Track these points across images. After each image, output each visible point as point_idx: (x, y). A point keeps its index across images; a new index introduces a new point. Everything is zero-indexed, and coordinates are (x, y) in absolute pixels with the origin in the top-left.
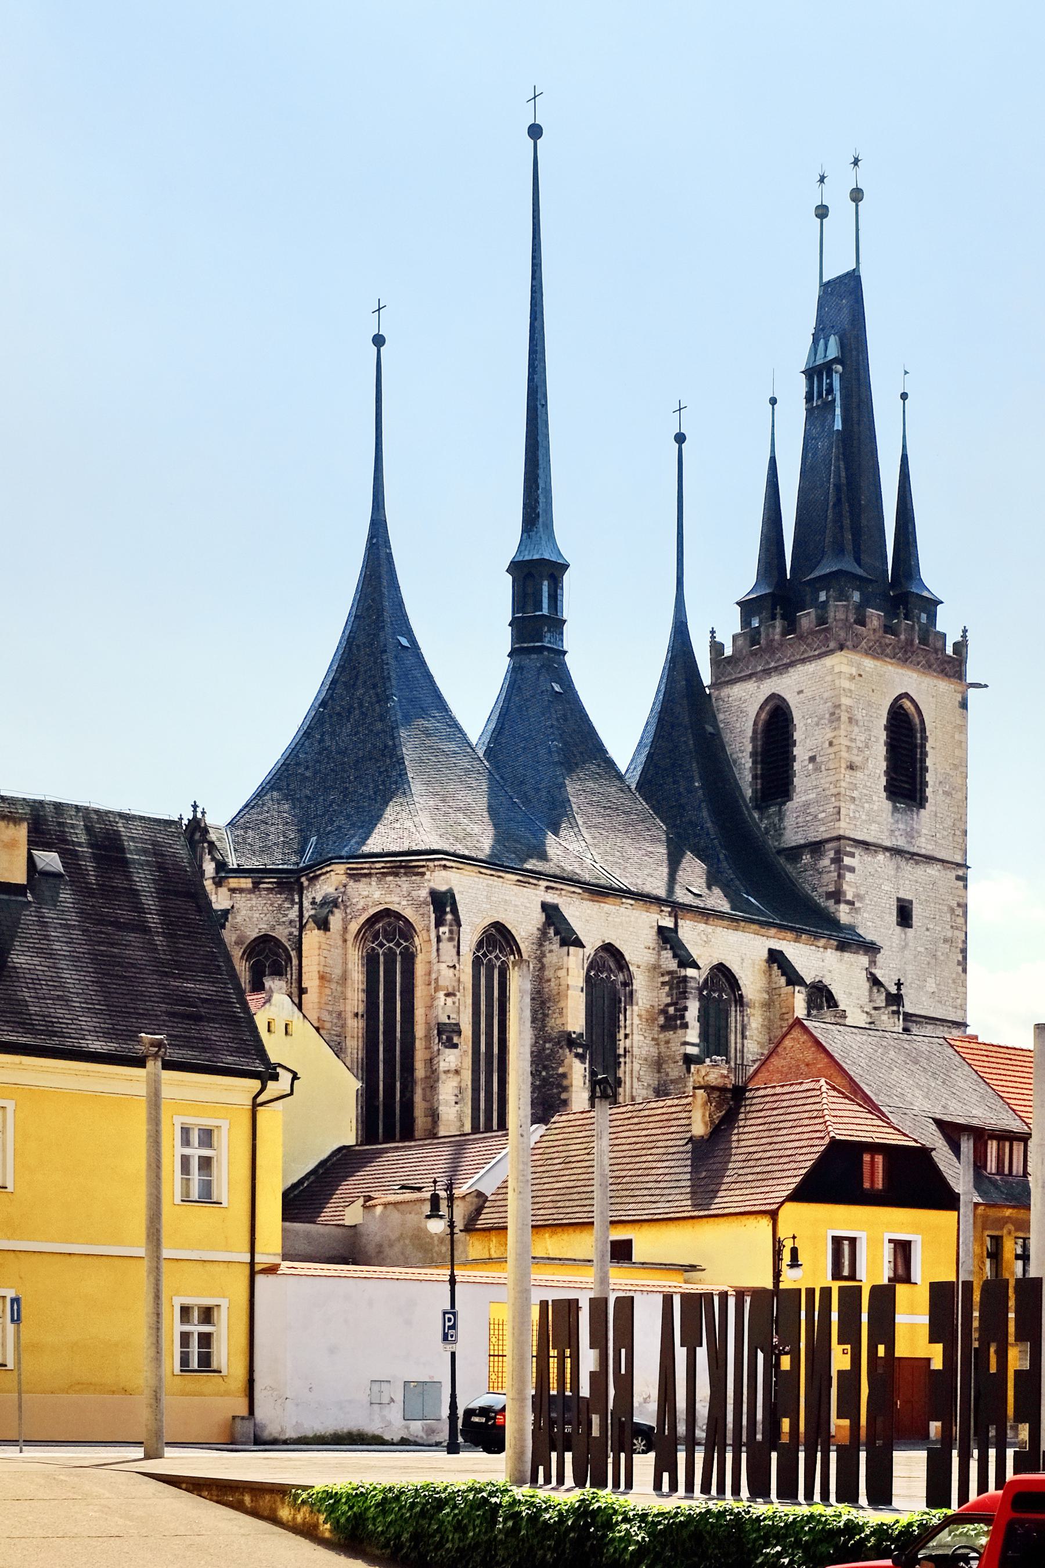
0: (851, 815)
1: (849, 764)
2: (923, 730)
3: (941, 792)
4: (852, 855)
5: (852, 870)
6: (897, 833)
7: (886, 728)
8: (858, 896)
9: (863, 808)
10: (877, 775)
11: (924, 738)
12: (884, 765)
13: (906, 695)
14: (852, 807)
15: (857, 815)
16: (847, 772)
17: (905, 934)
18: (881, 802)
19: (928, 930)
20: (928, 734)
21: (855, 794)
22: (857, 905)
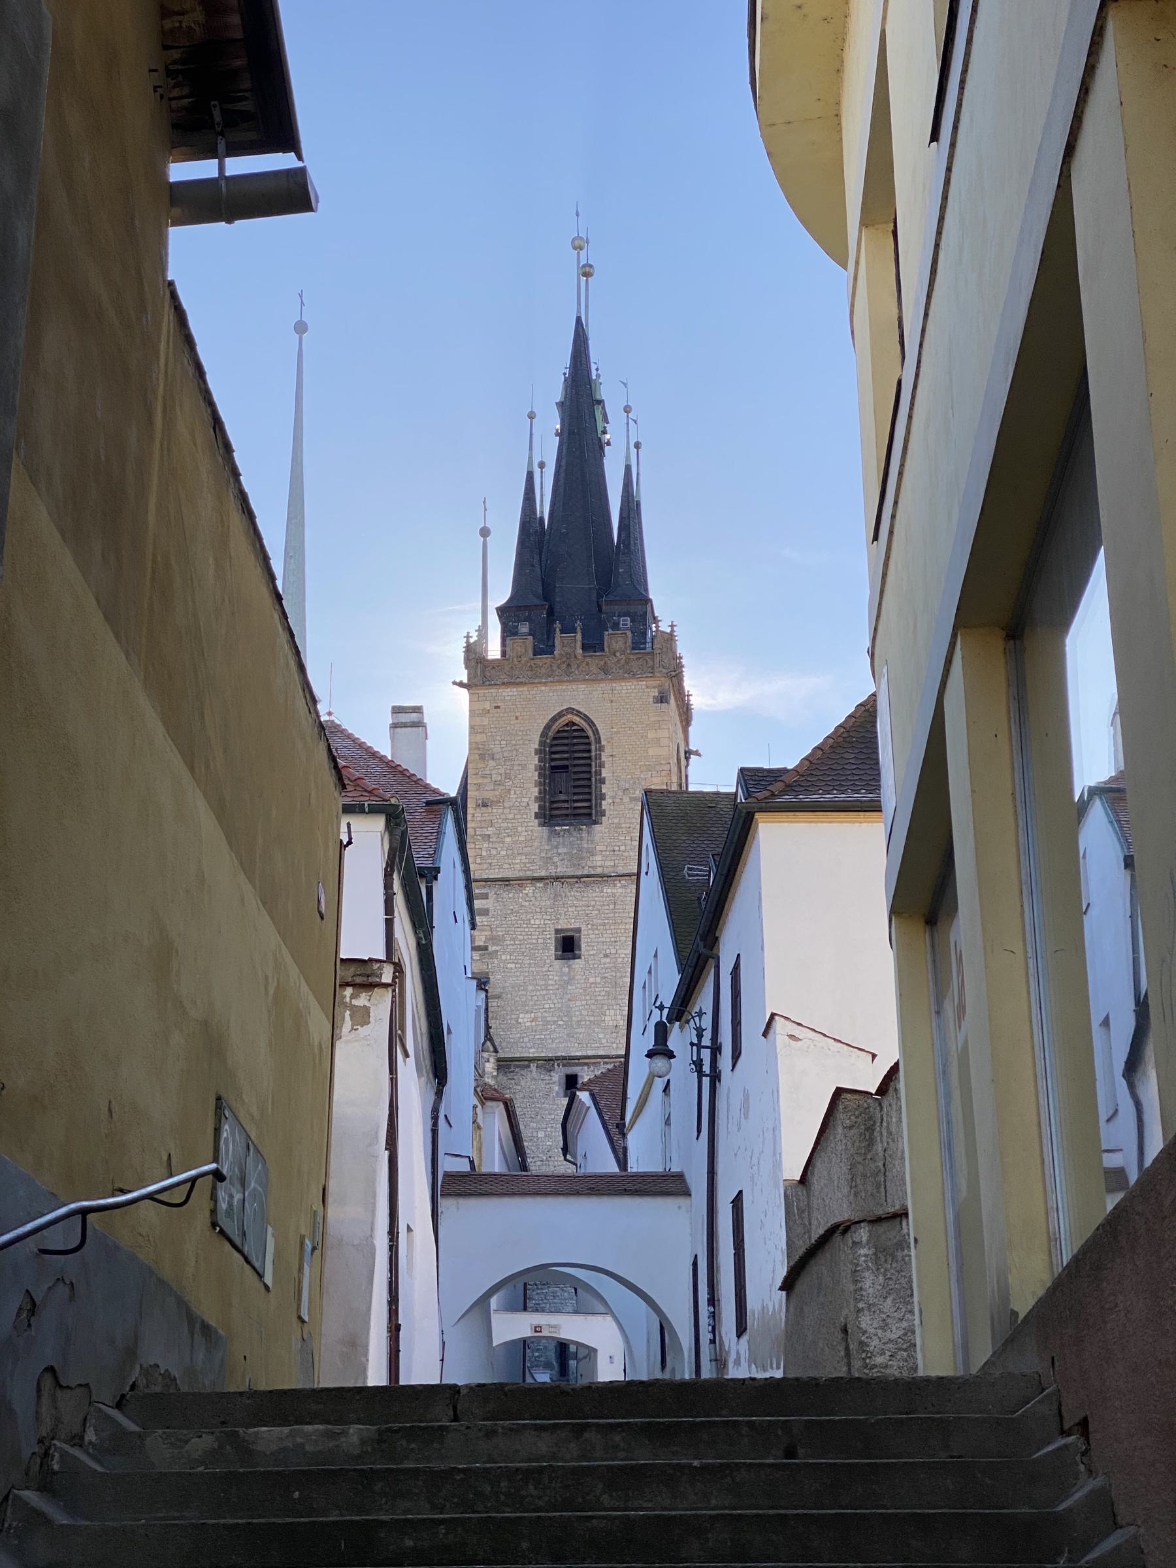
0: (484, 854)
1: (480, 802)
2: (598, 741)
3: (626, 800)
4: (485, 896)
5: (485, 912)
6: (556, 859)
7: (537, 752)
8: (494, 939)
9: (503, 842)
10: (525, 804)
11: (601, 749)
12: (535, 791)
13: (570, 710)
14: (486, 845)
15: (494, 852)
16: (478, 810)
17: (569, 967)
18: (530, 828)
19: (606, 956)
20: (603, 743)
21: (490, 831)
22: (491, 949)
